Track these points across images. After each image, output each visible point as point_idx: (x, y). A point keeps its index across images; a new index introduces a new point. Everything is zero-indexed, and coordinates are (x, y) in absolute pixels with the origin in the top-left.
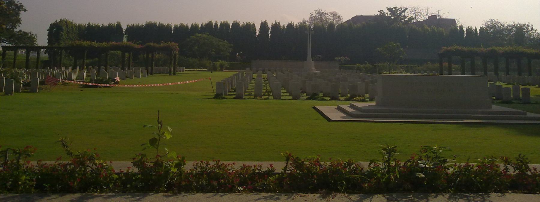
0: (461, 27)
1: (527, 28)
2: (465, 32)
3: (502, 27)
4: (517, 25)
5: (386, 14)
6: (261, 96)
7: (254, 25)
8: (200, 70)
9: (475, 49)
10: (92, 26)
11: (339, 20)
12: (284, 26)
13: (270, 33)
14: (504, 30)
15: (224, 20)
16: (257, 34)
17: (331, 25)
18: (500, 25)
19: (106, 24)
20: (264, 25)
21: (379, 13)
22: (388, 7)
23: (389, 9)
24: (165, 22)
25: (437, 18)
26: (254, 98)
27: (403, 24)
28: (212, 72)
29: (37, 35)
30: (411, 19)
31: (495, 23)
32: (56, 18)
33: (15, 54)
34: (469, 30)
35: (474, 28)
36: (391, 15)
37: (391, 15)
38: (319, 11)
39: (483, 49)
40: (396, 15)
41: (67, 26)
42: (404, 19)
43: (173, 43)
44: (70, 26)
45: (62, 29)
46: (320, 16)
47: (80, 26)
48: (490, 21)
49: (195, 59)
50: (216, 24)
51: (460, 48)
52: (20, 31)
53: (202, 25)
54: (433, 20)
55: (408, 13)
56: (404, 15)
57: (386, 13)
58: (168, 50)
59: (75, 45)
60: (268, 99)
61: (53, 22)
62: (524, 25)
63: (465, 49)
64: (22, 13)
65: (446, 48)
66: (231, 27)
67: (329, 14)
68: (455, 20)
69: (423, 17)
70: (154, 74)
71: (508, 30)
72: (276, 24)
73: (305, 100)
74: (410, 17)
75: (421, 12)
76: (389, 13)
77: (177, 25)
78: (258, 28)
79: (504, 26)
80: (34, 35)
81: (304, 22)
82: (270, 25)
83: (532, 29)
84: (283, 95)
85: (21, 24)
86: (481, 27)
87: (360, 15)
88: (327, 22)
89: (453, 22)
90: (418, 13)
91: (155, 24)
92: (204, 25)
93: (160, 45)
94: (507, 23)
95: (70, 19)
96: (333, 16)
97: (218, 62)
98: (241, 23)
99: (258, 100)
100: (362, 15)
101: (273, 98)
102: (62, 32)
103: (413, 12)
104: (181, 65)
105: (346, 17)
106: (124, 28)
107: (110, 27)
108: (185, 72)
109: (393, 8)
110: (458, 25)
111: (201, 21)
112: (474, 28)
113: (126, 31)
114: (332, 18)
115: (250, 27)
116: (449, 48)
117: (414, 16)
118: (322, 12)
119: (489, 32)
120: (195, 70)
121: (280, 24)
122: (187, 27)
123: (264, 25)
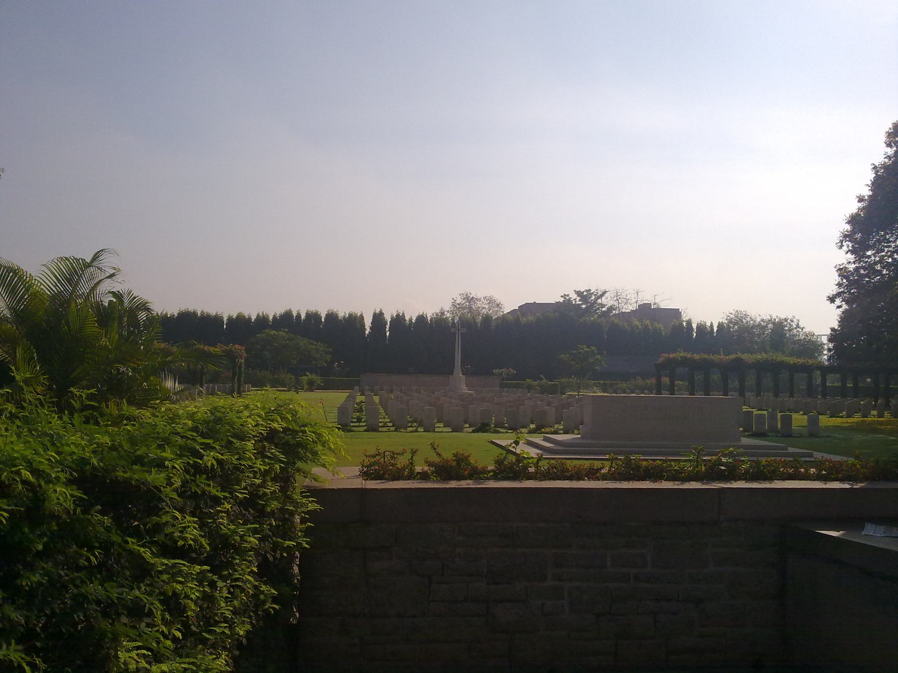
0: (689, 323)
1: (790, 324)
2: (695, 331)
3: (752, 322)
4: (775, 319)
5: (574, 301)
6: (406, 428)
7: (362, 317)
9: (712, 357)
11: (499, 309)
12: (411, 320)
13: (389, 330)
14: (754, 327)
16: (367, 332)
17: (487, 319)
18: (748, 319)
20: (378, 318)
21: (562, 300)
22: (577, 290)
23: (579, 293)
25: (652, 307)
27: (599, 317)
30: (611, 309)
31: (742, 315)
34: (701, 328)
35: (708, 324)
36: (580, 303)
37: (580, 303)
38: (467, 295)
39: (722, 357)
40: (589, 303)
42: (601, 309)
46: (468, 304)
48: (734, 312)
51: (689, 356)
54: (645, 310)
55: (607, 299)
56: (600, 302)
57: (574, 299)
62: (786, 320)
63: (696, 357)
65: (668, 355)
66: (323, 320)
67: (482, 299)
68: (680, 311)
69: (631, 305)
71: (761, 327)
72: (398, 315)
74: (611, 306)
75: (627, 298)
76: (578, 298)
78: (368, 322)
79: (755, 322)
81: (443, 314)
83: (798, 326)
86: (719, 322)
87: (533, 302)
88: (479, 314)
89: (676, 313)
90: (623, 300)
94: (760, 316)
96: (489, 303)
98: (341, 315)
99: (400, 433)
100: (535, 302)
103: (615, 299)
105: (510, 304)
109: (584, 292)
110: (685, 317)
112: (708, 324)
114: (487, 306)
115: (354, 321)
116: (671, 356)
117: (616, 303)
118: (471, 296)
119: (732, 330)
121: (404, 316)
123: (378, 318)
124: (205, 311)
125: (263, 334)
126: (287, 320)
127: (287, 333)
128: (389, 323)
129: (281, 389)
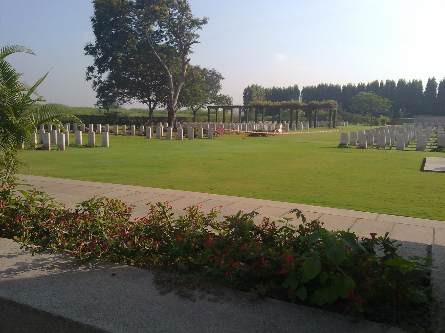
7: (421, 82)
8: (362, 124)
10: (276, 89)
13: (438, 90)
15: (390, 79)
16: (424, 91)
19: (286, 87)
24: (335, 83)
26: (376, 149)
28: (371, 126)
29: (233, 98)
32: (249, 84)
33: (232, 112)
41: (257, 90)
43: (333, 101)
44: (259, 90)
45: (253, 92)
47: (267, 89)
49: (359, 115)
50: (382, 83)
52: (221, 95)
53: (368, 84)
58: (327, 107)
59: (255, 104)
60: (390, 149)
61: (246, 87)
64: (221, 82)
66: (396, 85)
70: (317, 127)
73: (430, 152)
77: (345, 85)
78: (424, 85)
80: (231, 97)
82: (438, 82)
84: (412, 146)
85: (221, 89)
91: (326, 85)
92: (370, 84)
93: (321, 103)
95: (259, 84)
97: (380, 118)
101: (396, 149)
102: (253, 94)
104: (345, 120)
106: (301, 89)
107: (290, 89)
108: (348, 126)
111: (367, 81)
113: (302, 92)
115: (416, 85)
120: (359, 124)
122: (355, 86)
124: (331, 84)
125: (359, 94)
126: (374, 86)
127: (373, 93)
128: (438, 85)
129: (366, 124)
